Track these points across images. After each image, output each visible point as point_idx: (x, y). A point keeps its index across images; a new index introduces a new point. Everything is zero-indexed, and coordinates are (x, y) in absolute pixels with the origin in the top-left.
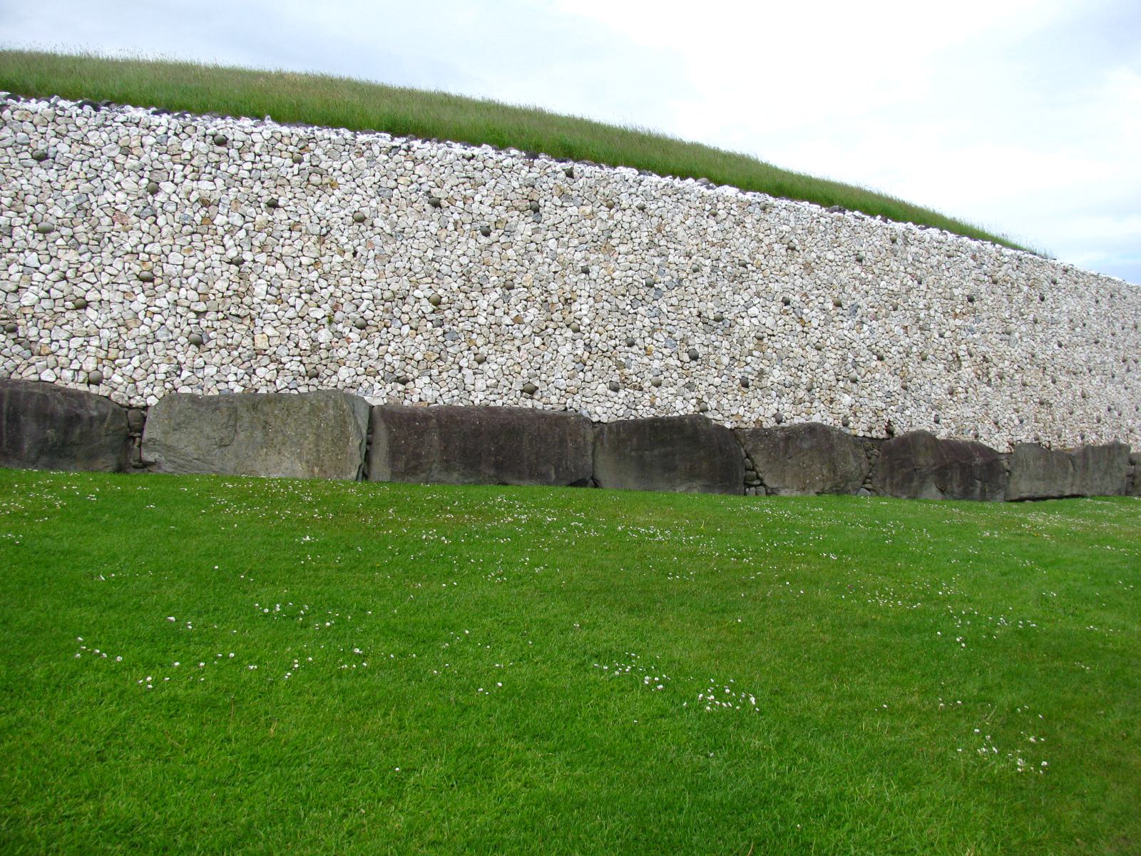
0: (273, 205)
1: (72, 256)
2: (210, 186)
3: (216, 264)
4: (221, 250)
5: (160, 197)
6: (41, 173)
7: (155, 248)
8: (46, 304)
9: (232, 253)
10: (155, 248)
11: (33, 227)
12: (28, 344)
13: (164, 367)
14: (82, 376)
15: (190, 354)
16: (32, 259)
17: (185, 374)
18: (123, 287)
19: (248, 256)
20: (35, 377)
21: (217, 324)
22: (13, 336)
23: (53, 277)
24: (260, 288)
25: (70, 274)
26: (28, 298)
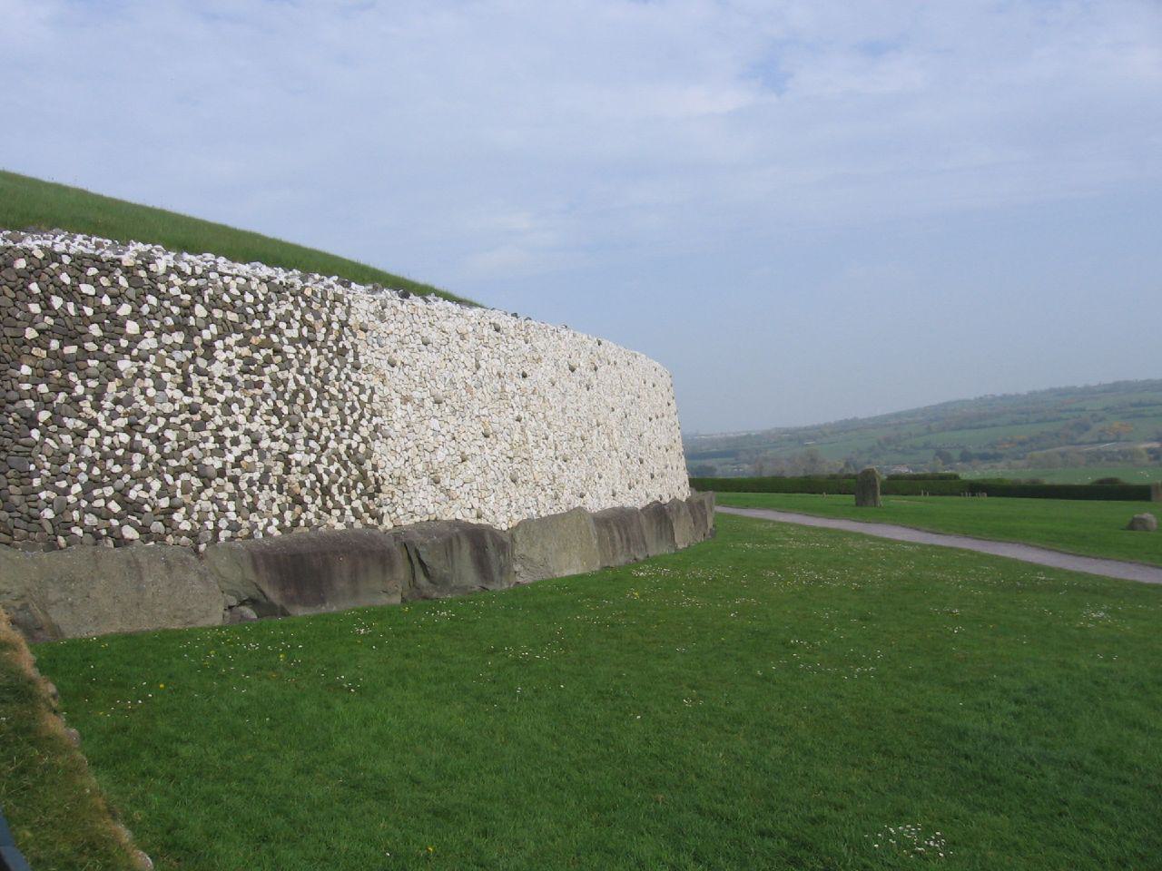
0: (524, 376)
1: (452, 420)
2: (498, 362)
3: (512, 422)
4: (510, 410)
5: (480, 373)
6: (428, 357)
7: (485, 412)
8: (449, 459)
9: (516, 414)
10: (485, 412)
11: (432, 398)
12: (447, 491)
13: (506, 502)
14: (474, 513)
15: (513, 490)
16: (435, 424)
17: (513, 504)
18: (479, 443)
19: (522, 415)
20: (453, 518)
21: (519, 467)
22: (439, 486)
23: (449, 437)
24: (531, 438)
25: (456, 435)
26: (441, 454)
